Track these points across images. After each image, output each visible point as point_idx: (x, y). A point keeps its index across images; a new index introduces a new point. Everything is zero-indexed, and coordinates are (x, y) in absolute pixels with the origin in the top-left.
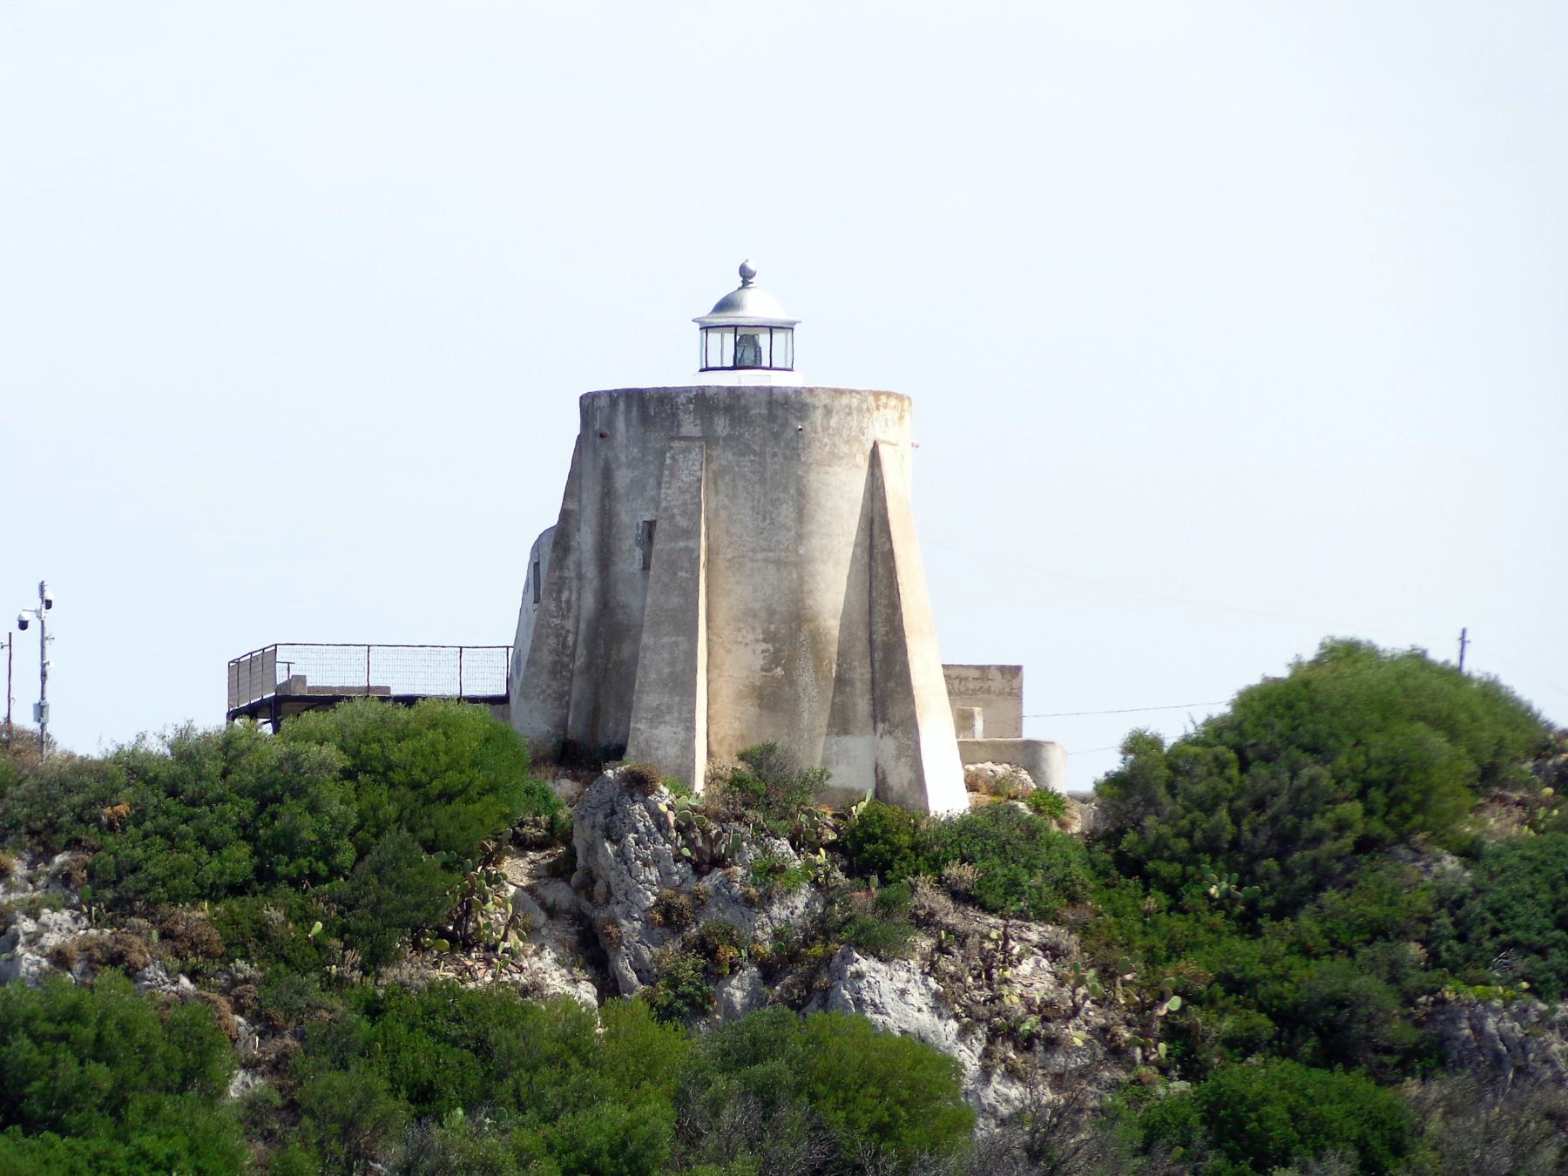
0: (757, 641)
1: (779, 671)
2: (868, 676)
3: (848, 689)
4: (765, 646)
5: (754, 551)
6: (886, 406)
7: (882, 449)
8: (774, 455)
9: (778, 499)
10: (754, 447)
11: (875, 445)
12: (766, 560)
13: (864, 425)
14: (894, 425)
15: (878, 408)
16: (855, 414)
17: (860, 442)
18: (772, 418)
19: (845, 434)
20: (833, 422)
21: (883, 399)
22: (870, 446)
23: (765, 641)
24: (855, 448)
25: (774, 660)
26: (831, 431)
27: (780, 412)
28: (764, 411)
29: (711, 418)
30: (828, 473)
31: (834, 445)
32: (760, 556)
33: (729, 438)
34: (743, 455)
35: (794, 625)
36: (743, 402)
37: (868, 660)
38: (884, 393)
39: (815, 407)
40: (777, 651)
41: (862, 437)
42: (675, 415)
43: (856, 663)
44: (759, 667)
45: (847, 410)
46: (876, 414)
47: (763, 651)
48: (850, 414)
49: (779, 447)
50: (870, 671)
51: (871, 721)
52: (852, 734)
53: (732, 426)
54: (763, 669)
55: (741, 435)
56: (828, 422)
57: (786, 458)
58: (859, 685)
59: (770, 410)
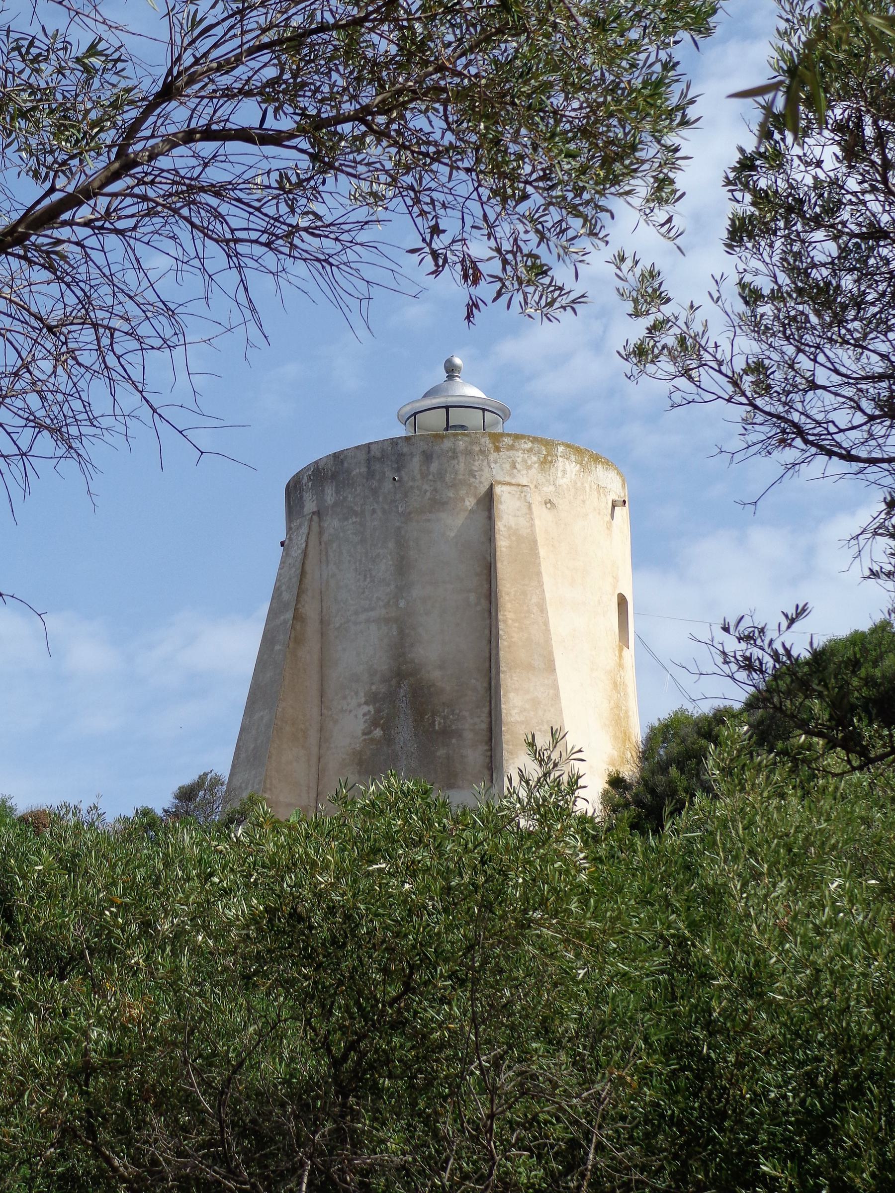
0: (359, 705)
1: (378, 733)
2: (484, 726)
3: (454, 741)
4: (366, 709)
5: (356, 613)
6: (511, 448)
7: (498, 490)
8: (374, 511)
9: (378, 555)
10: (356, 508)
11: (491, 487)
12: (368, 621)
13: (475, 468)
14: (529, 468)
15: (498, 449)
16: (462, 459)
17: (470, 485)
18: (370, 474)
19: (448, 478)
20: (434, 467)
21: (507, 440)
22: (483, 489)
23: (366, 703)
24: (462, 492)
25: (375, 723)
26: (431, 477)
27: (377, 466)
28: (364, 469)
29: (323, 491)
30: (429, 520)
31: (435, 490)
32: (363, 617)
33: (335, 504)
34: (346, 519)
35: (394, 682)
36: (346, 465)
37: (486, 710)
38: (509, 435)
39: (412, 455)
40: (378, 711)
41: (472, 480)
42: (301, 497)
43: (466, 714)
44: (360, 733)
45: (450, 454)
46: (493, 456)
47: (364, 715)
48: (455, 456)
49: (377, 503)
50: (486, 720)
51: (486, 772)
52: (459, 787)
53: (337, 492)
54: (364, 734)
55: (345, 498)
56: (428, 468)
57: (384, 512)
58: (468, 735)
59: (369, 467)
